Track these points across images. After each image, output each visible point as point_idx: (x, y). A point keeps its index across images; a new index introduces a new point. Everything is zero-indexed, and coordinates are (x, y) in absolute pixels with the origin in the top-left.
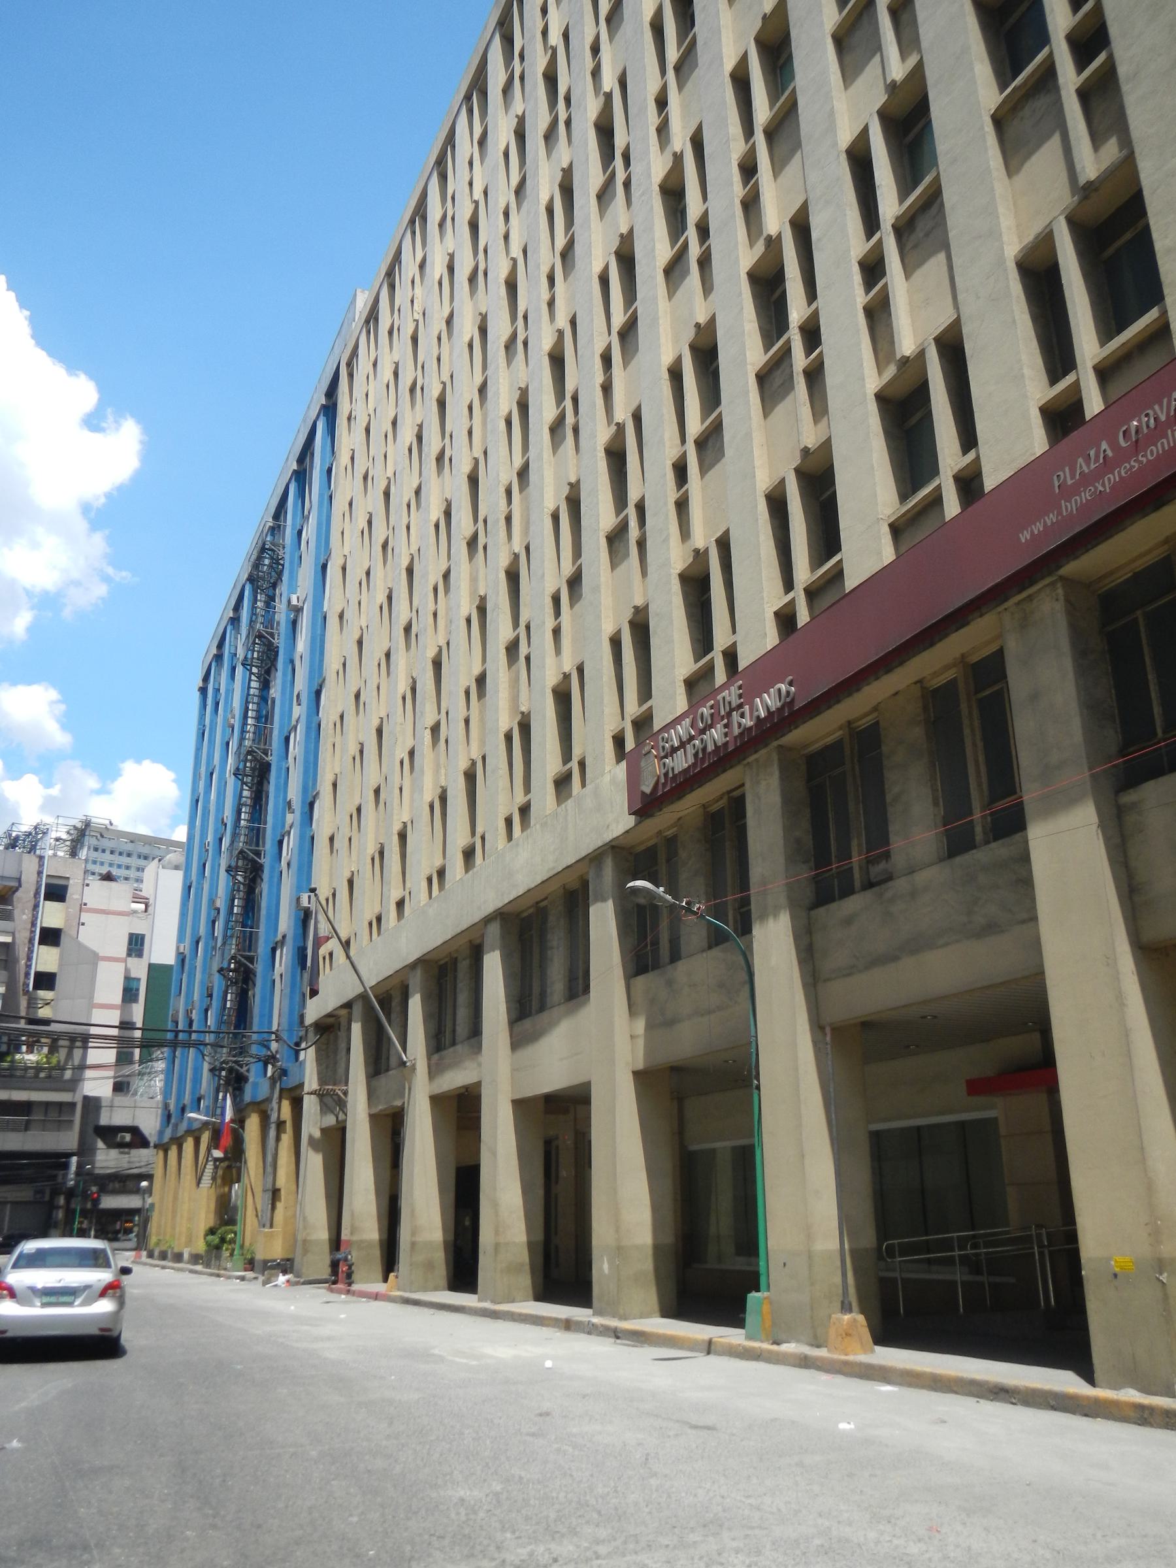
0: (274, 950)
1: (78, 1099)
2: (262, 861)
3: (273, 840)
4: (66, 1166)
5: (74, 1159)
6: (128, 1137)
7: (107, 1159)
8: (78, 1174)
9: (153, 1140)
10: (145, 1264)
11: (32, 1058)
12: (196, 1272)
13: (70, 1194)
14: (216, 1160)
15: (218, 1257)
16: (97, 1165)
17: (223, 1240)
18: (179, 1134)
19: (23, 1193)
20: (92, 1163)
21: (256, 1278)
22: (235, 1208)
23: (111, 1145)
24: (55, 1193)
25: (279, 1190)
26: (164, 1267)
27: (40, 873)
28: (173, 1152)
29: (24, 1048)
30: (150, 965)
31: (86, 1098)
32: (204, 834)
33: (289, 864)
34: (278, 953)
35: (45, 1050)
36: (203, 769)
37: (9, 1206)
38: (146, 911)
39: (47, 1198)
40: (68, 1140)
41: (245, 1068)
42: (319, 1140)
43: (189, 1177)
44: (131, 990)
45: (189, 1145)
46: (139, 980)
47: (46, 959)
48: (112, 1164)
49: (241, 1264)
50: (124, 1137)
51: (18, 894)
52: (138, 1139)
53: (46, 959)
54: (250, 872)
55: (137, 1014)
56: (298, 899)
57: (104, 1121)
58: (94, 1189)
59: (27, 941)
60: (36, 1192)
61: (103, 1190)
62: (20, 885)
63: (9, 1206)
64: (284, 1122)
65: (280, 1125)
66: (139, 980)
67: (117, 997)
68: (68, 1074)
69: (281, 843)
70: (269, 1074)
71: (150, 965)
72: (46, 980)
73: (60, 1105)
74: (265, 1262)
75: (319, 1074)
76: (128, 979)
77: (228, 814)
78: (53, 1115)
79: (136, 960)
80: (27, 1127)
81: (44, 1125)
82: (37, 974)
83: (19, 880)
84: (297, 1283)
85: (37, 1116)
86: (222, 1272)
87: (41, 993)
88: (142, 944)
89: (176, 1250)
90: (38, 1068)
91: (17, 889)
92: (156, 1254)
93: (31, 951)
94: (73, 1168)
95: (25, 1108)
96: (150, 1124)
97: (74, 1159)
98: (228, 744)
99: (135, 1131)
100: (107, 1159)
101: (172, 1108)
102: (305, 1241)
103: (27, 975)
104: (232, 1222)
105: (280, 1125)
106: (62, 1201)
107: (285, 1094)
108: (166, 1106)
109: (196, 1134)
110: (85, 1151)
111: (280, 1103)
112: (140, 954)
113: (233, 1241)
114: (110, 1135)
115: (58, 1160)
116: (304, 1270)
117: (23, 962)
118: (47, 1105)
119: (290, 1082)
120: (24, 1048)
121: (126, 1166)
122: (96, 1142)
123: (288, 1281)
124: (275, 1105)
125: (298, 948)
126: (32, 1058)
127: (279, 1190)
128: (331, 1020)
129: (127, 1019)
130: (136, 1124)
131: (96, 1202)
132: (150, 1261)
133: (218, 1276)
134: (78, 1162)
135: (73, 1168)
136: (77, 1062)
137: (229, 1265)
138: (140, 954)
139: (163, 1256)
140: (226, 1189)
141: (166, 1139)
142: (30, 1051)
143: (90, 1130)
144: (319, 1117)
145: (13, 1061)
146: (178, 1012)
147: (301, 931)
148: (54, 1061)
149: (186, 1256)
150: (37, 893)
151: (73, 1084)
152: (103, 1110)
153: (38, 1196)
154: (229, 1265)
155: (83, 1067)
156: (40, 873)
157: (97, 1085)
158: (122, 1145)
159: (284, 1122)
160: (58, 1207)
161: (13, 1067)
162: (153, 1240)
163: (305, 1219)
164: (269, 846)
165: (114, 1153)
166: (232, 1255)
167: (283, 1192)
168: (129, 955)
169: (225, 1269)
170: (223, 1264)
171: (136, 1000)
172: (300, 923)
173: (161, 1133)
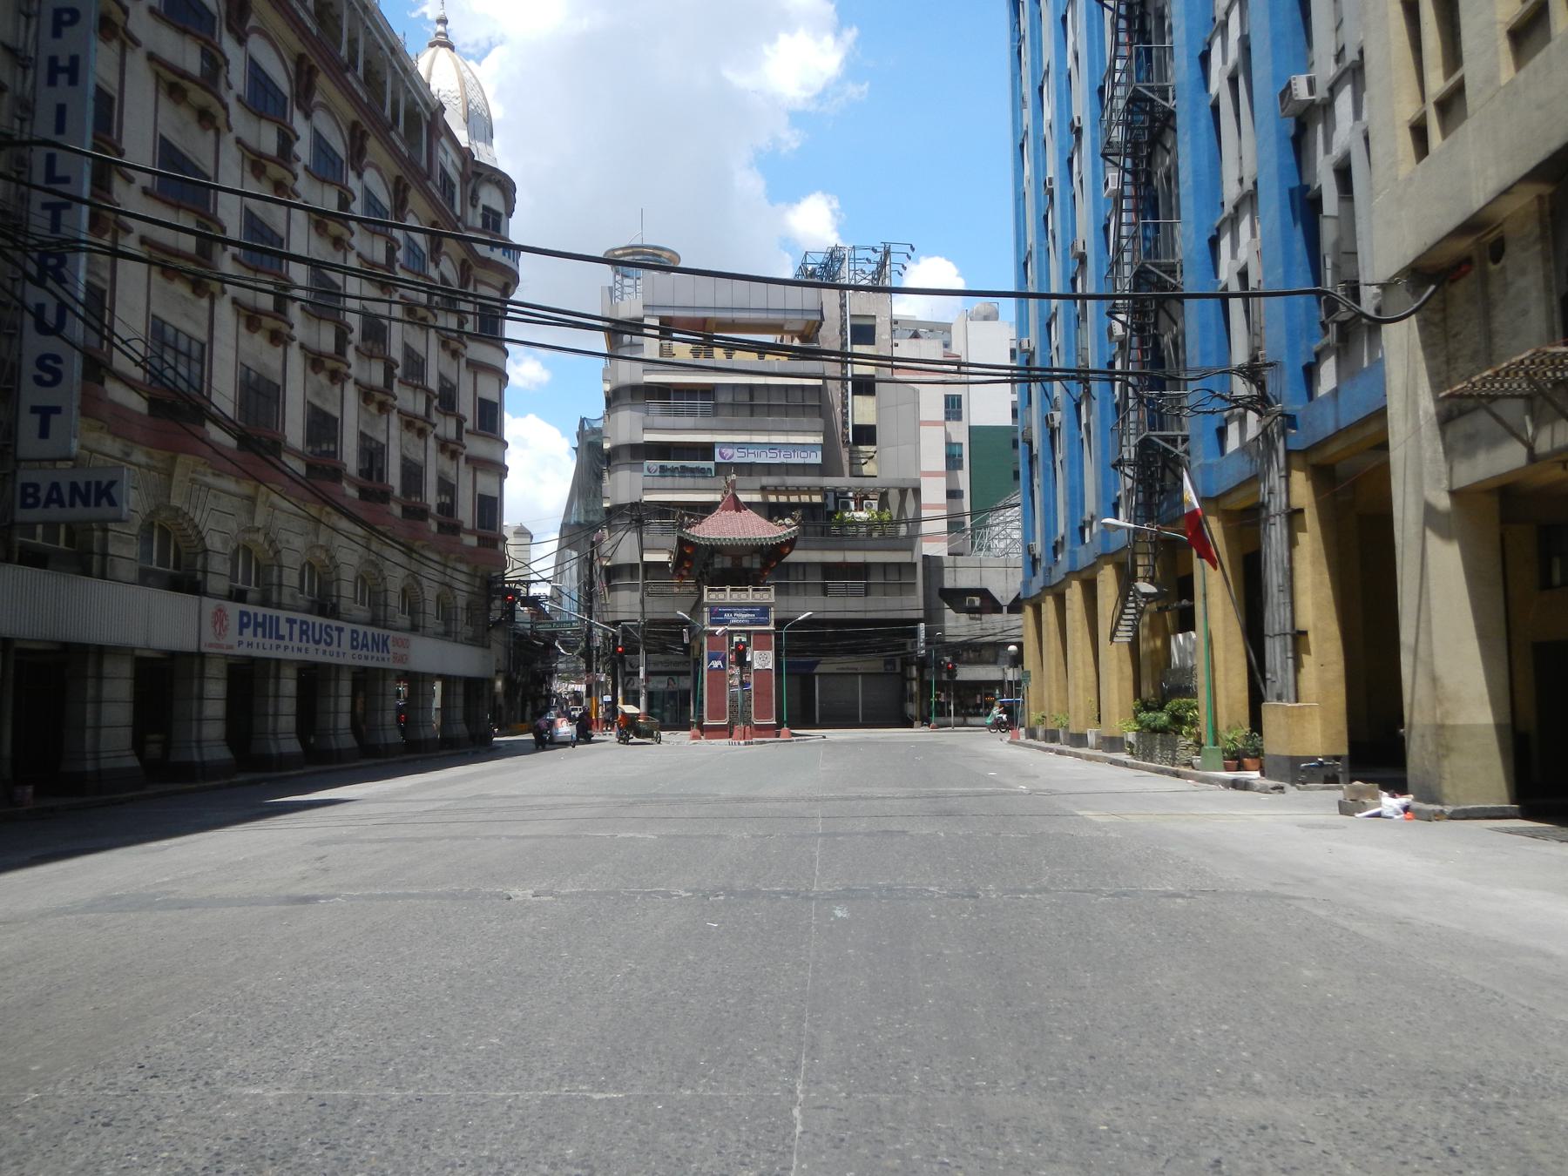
0: (1214, 243)
2: (1170, 104)
3: (1190, 56)
4: (914, 634)
5: (922, 625)
6: (977, 601)
7: (957, 625)
8: (927, 643)
10: (1030, 746)
11: (862, 515)
12: (1126, 765)
13: (923, 664)
14: (1145, 595)
15: (1173, 748)
16: (948, 632)
17: (1178, 720)
18: (1054, 582)
19: (873, 664)
20: (942, 630)
21: (1280, 789)
22: (1188, 672)
24: (906, 663)
25: (1305, 633)
26: (1059, 753)
27: (843, 306)
28: (1049, 607)
29: (852, 504)
31: (925, 557)
32: (1040, 166)
33: (1233, 81)
34: (1225, 244)
35: (875, 504)
36: (1028, 90)
39: (898, 669)
40: (911, 604)
41: (1181, 448)
42: (1447, 515)
43: (1079, 634)
45: (1074, 594)
47: (863, 410)
48: (963, 631)
49: (1218, 759)
51: (822, 332)
52: (989, 603)
53: (863, 410)
54: (1145, 135)
55: (963, 479)
56: (1286, 92)
58: (948, 659)
60: (886, 663)
61: (957, 659)
62: (823, 319)
64: (1301, 511)
65: (1293, 516)
67: (941, 465)
68: (903, 530)
69: (1205, 58)
70: (1233, 442)
72: (866, 434)
74: (1294, 761)
75: (1431, 376)
76: (949, 444)
77: (1082, 107)
78: (893, 578)
79: (955, 423)
81: (886, 589)
82: (854, 427)
83: (821, 312)
84: (1439, 816)
86: (1182, 769)
87: (862, 448)
88: (960, 406)
89: (1073, 730)
90: (868, 523)
91: (820, 325)
92: (1040, 733)
93: (845, 405)
94: (922, 636)
95: (862, 570)
96: (1005, 586)
97: (922, 625)
98: (1064, 18)
99: (984, 593)
100: (957, 625)
101: (1038, 549)
102: (1440, 728)
103: (845, 423)
104: (1189, 692)
105: (1293, 516)
107: (1295, 460)
108: (1029, 550)
109: (1085, 575)
110: (932, 616)
111: (1288, 477)
112: (959, 417)
113: (1194, 723)
114: (957, 598)
115: (906, 628)
116: (1447, 789)
119: (1300, 439)
120: (852, 504)
121: (979, 632)
123: (1406, 809)
124: (1275, 479)
125: (1292, 191)
126: (862, 515)
127: (1305, 633)
128: (1464, 245)
129: (954, 487)
130: (984, 586)
131: (952, 673)
132: (1031, 741)
133: (1177, 775)
135: (922, 636)
136: (910, 516)
137: (1197, 760)
138: (959, 417)
139: (1052, 736)
140: (1159, 643)
141: (1035, 589)
142: (860, 508)
143: (935, 594)
144: (1443, 467)
145: (842, 518)
146: (1030, 427)
147: (1291, 160)
148: (886, 517)
149: (1091, 739)
150: (843, 330)
151: (909, 543)
154: (1197, 760)
155: (918, 520)
156: (843, 306)
157: (935, 548)
158: (971, 610)
159: (1301, 511)
161: (843, 524)
162: (1034, 716)
163: (1434, 680)
164: (1180, 70)
165: (964, 617)
166: (1198, 743)
167: (1311, 636)
168: (947, 419)
169: (1189, 764)
170: (1183, 756)
171: (961, 468)
172: (1289, 145)
173: (1026, 584)
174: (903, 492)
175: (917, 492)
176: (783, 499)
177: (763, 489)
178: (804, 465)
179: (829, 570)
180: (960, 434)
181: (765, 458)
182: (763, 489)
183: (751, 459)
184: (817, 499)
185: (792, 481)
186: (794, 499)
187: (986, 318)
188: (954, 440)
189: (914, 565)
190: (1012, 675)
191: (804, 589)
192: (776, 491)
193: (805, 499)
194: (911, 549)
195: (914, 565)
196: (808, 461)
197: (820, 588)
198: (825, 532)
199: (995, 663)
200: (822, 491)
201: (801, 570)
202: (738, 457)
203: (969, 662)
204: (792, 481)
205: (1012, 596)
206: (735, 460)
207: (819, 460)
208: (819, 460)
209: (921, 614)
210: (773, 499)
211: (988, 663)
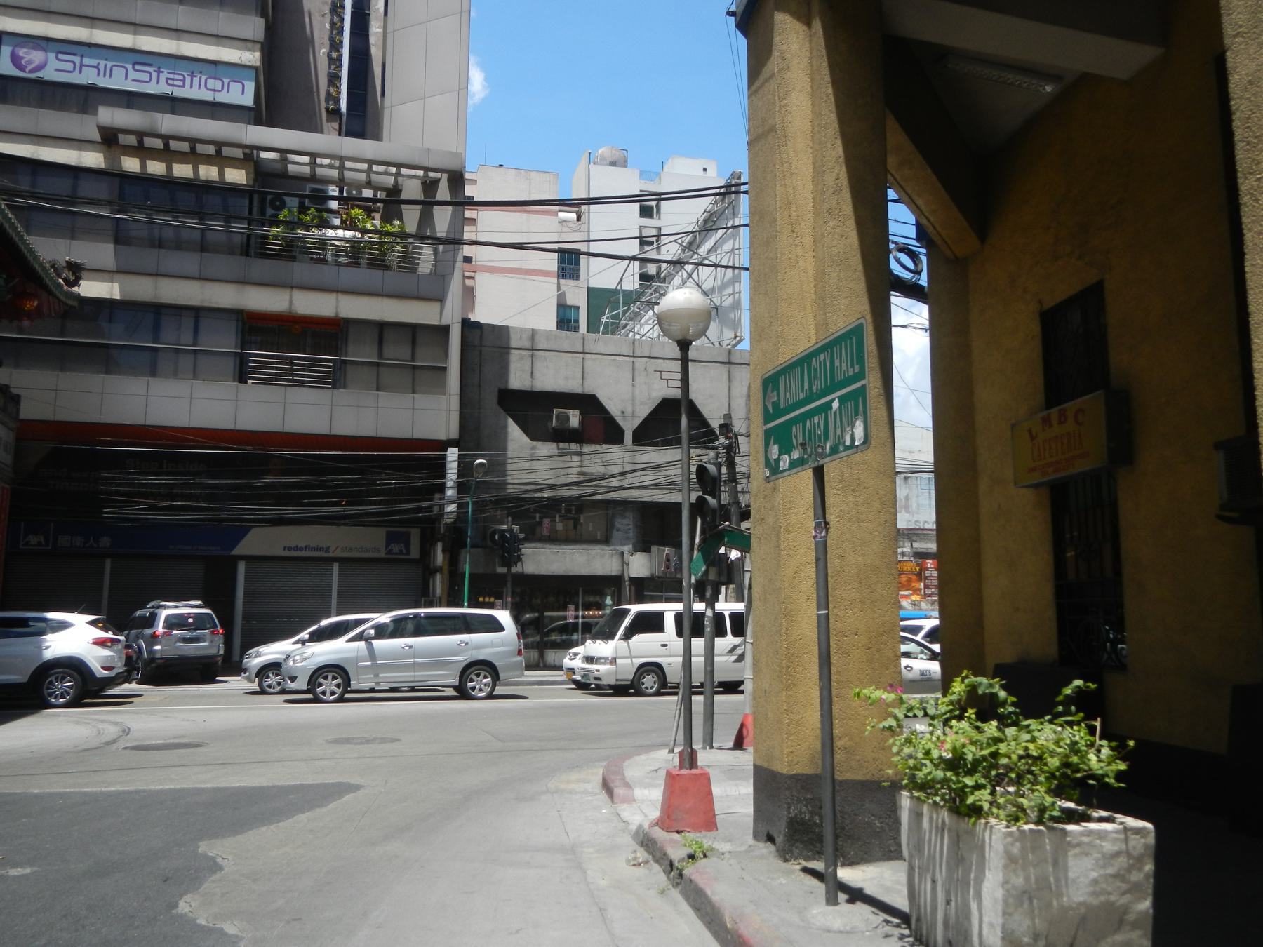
1: (451, 315)
5: (453, 453)
6: (574, 419)
7: (530, 462)
8: (461, 487)
9: (629, 426)
13: (456, 540)
19: (369, 541)
20: (498, 465)
23: (536, 432)
30: (589, 290)
37: (336, 567)
38: (579, 219)
39: (415, 553)
44: (569, 321)
46: (578, 308)
50: (568, 418)
52: (598, 424)
57: (517, 381)
59: (327, 9)
60: (391, 538)
61: (533, 535)
63: (336, 567)
66: (578, 308)
71: (590, 291)
73: (413, 332)
78: (397, 352)
79: (571, 282)
80: (336, 379)
81: (380, 377)
85: (360, 352)
95: (329, 334)
97: (453, 453)
99: (588, 403)
100: (530, 462)
103: (334, 78)
106: (440, 558)
115: (421, 458)
117: (322, 52)
118: (382, 329)
122: (505, 427)
130: (589, 388)
131: (508, 551)
134: (461, 459)
138: (577, 277)
143: (490, 399)
152: (514, 355)
153: (395, 548)
158: (562, 435)
160: (439, 570)
165: (547, 448)
174: (430, 186)
175: (457, 179)
176: (156, 168)
177: (109, 139)
178: (214, 105)
179: (255, 328)
180: (577, 296)
181: (121, 79)
182: (109, 139)
183: (87, 77)
184: (236, 176)
185: (168, 123)
186: (182, 171)
187: (613, 164)
188: (570, 302)
189: (444, 330)
190: (639, 565)
191: (194, 364)
192: (141, 151)
193: (209, 172)
194: (441, 300)
195: (444, 330)
196: (222, 98)
197: (230, 365)
198: (254, 248)
199: (606, 541)
200: (249, 157)
201: (188, 322)
202: (55, 69)
203: (554, 539)
204: (168, 123)
205: (644, 411)
206: (49, 74)
207: (248, 99)
208: (248, 99)
209: (454, 433)
210: (131, 164)
211: (593, 541)
